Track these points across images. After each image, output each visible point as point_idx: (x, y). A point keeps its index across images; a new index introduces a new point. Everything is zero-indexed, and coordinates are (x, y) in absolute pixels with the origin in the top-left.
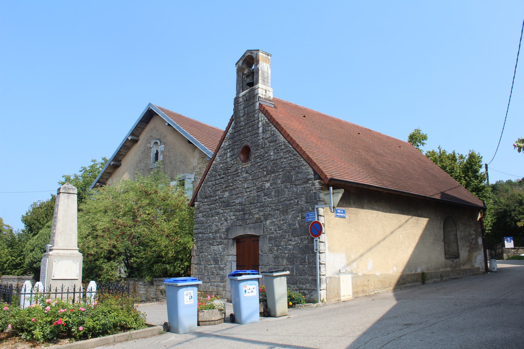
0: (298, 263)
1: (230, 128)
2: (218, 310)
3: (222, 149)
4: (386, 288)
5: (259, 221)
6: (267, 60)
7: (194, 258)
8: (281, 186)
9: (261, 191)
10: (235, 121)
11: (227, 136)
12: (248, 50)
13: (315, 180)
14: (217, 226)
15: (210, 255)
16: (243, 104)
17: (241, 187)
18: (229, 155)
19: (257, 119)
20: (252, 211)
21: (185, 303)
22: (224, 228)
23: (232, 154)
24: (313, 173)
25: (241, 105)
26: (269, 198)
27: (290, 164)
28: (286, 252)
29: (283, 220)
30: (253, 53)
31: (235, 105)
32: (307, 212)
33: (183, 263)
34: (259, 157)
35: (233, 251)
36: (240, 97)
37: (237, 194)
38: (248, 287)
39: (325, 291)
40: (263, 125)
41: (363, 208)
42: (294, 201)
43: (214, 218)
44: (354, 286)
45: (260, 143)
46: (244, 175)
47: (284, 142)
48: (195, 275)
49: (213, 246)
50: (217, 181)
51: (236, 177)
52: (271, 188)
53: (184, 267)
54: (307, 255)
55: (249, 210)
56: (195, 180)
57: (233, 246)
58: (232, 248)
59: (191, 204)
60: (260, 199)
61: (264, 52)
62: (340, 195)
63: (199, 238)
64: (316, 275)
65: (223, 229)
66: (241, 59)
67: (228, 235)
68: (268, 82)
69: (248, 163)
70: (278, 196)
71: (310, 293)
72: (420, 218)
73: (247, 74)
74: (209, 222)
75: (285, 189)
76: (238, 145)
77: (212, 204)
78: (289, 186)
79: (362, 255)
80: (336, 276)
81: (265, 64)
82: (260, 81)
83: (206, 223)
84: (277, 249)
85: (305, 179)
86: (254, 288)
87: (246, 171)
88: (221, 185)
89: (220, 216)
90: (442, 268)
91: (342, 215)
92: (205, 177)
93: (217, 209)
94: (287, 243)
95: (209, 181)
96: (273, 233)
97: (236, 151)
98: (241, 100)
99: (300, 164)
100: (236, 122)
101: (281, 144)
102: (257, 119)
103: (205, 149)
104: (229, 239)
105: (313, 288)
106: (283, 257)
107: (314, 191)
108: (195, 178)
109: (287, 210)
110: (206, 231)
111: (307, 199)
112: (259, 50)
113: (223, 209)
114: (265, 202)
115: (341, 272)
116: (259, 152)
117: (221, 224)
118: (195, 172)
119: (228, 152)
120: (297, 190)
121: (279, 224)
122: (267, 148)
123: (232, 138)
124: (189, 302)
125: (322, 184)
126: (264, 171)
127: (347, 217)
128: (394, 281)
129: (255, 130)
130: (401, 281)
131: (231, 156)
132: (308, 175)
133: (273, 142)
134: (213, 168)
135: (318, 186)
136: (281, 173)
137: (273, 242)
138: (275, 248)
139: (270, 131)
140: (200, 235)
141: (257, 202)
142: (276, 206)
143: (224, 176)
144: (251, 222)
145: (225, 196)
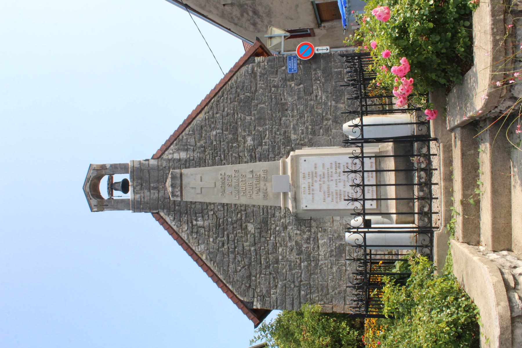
7: (335, 305)
9: (255, 153)
14: (292, 250)
15: (331, 268)
22: (295, 232)
26: (266, 135)
29: (293, 110)
32: (287, 72)
43: (280, 257)
47: (205, 114)
54: (333, 69)
60: (264, 153)
75: (258, 108)
77: (261, 263)
78: (256, 102)
89: (278, 241)
95: (228, 271)
96: (307, 128)
99: (234, 86)
106: (336, 107)
107: (266, 64)
110: (297, 278)
111: (272, 73)
122: (206, 142)
123: (181, 213)
126: (232, 146)
132: (248, 71)
136: (240, 115)
138: (325, 122)
145: (253, 231)
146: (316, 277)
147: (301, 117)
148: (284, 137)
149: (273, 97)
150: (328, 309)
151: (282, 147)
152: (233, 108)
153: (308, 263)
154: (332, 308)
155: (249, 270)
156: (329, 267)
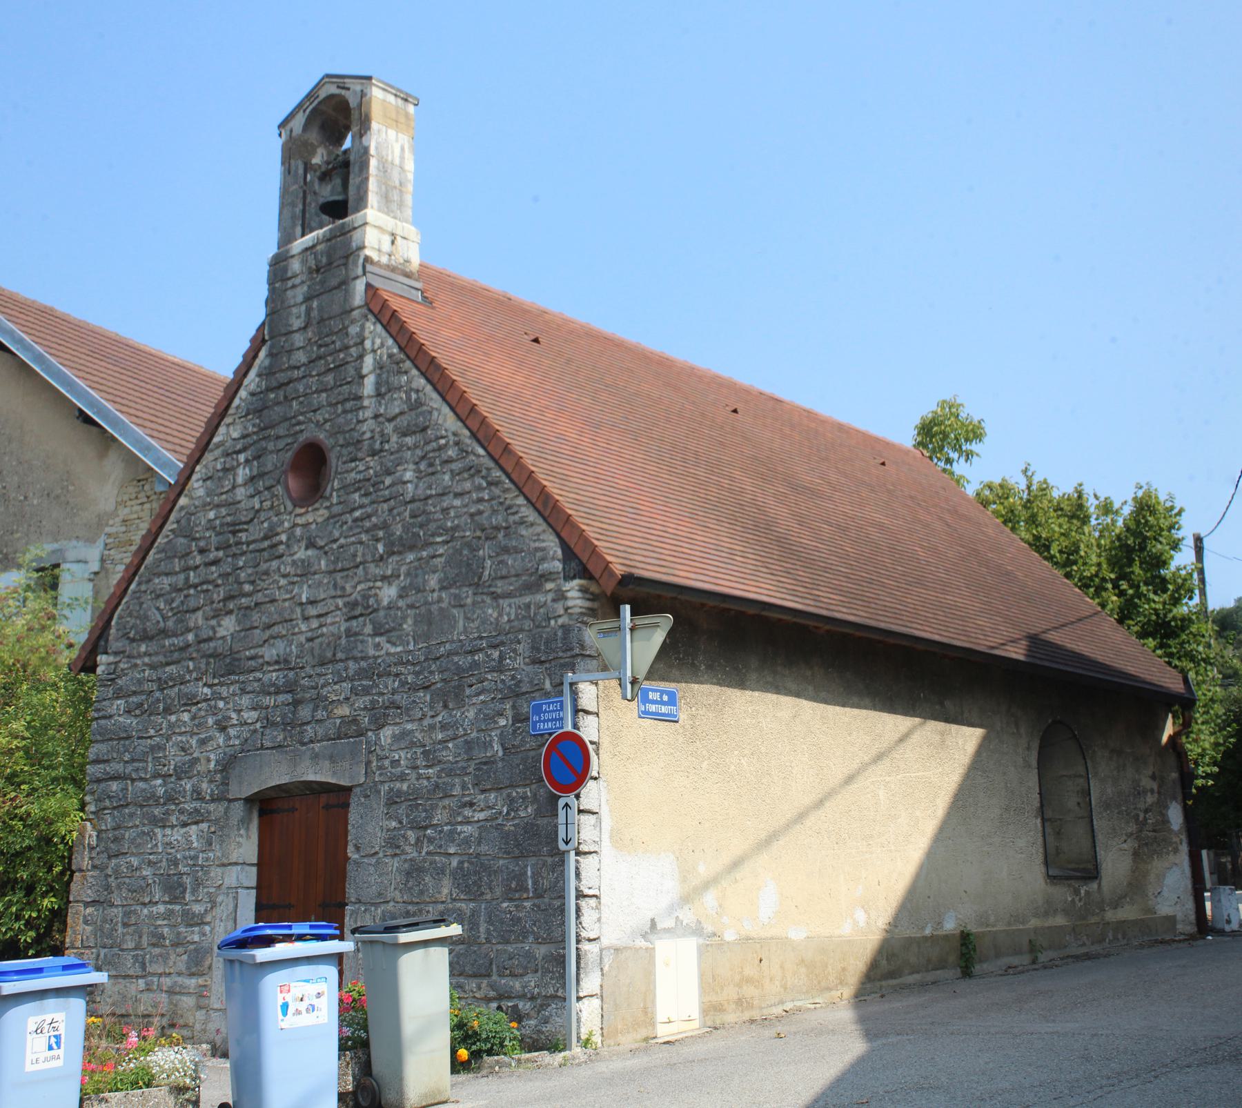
0: (498, 891)
1: (253, 374)
2: (167, 1088)
3: (218, 452)
4: (829, 989)
5: (351, 730)
6: (402, 119)
7: (84, 877)
8: (440, 600)
9: (361, 615)
10: (271, 347)
11: (236, 402)
12: (328, 76)
13: (568, 578)
14: (183, 749)
15: (150, 863)
16: (303, 282)
17: (285, 600)
18: (242, 474)
19: (356, 345)
20: (324, 692)
21: (29, 1068)
22: (212, 757)
23: (255, 473)
24: (559, 552)
25: (294, 286)
26: (394, 644)
27: (476, 518)
28: (452, 851)
29: (444, 727)
30: (348, 89)
31: (271, 283)
32: (534, 699)
33: (35, 900)
34: (359, 489)
35: (246, 846)
36: (293, 256)
37: (269, 627)
38: (298, 989)
39: (596, 1002)
40: (379, 366)
41: (742, 685)
42: (488, 656)
43: (173, 718)
44: (708, 982)
45: (364, 433)
46: (301, 554)
47: (455, 434)
48: (84, 947)
49: (164, 827)
50: (192, 574)
51: (266, 561)
52: (401, 603)
53: (38, 917)
54: (532, 860)
55: (313, 688)
56: (102, 567)
57: (247, 829)
58: (242, 836)
59: (80, 665)
60: (359, 644)
61: (392, 87)
62: (658, 638)
63: (109, 797)
64: (562, 941)
65: (209, 760)
66: (299, 106)
67: (227, 784)
68: (401, 205)
69: (317, 509)
70: (427, 637)
71: (539, 1012)
72: (954, 727)
73: (323, 169)
74: (152, 732)
75: (455, 611)
76: (278, 437)
77: (168, 664)
78: (469, 601)
79: (736, 864)
80: (641, 943)
81: (392, 133)
82: (373, 198)
83: (139, 738)
84: (418, 839)
85: (531, 575)
86: (319, 995)
87: (309, 539)
88: (207, 591)
89: (200, 709)
90: (1036, 915)
91: (664, 709)
92: (144, 558)
93: (189, 681)
94: (454, 813)
95: (159, 575)
96: (402, 778)
97: (271, 461)
98: (296, 266)
99: (511, 518)
100: (275, 351)
101: (443, 442)
102: (356, 345)
103: (147, 449)
104: (230, 801)
105: (551, 991)
106: (440, 872)
107: (560, 621)
108: (103, 560)
109: (460, 688)
110: (137, 770)
111: (535, 648)
112: (369, 78)
113: (210, 682)
114: (376, 658)
115: (659, 926)
116: (361, 468)
117: (203, 742)
118: (103, 537)
119: (239, 465)
120: (500, 615)
121: (427, 741)
122: (392, 454)
123: (258, 412)
124: (46, 1060)
125: (592, 594)
126: (378, 540)
127: (682, 717)
128: (857, 965)
129: (349, 383)
130: (884, 962)
131: (252, 479)
132: (543, 559)
133: (414, 433)
134: (178, 522)
135: (579, 602)
136: (441, 551)
137: (402, 810)
138: (411, 835)
139: (406, 392)
140: (115, 786)
141: (347, 659)
142: (417, 674)
143: (221, 554)
144: (321, 732)
145: (221, 632)
146: (137, 823)
147: (426, 754)
148: (387, 704)
149: (476, 658)
150: (79, 859)
151: (367, 698)
152: (458, 526)
153: (160, 797)
154: (81, 870)
155: (157, 635)
156: (151, 857)
